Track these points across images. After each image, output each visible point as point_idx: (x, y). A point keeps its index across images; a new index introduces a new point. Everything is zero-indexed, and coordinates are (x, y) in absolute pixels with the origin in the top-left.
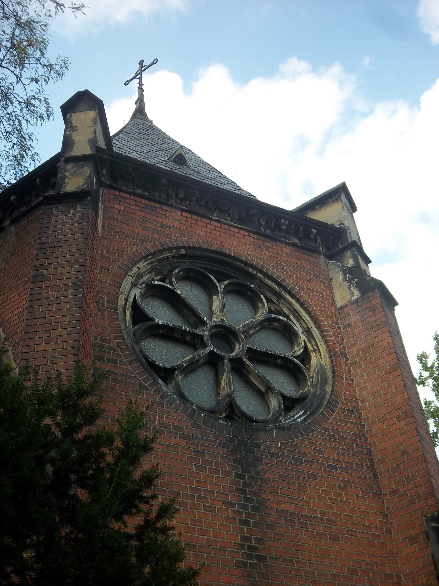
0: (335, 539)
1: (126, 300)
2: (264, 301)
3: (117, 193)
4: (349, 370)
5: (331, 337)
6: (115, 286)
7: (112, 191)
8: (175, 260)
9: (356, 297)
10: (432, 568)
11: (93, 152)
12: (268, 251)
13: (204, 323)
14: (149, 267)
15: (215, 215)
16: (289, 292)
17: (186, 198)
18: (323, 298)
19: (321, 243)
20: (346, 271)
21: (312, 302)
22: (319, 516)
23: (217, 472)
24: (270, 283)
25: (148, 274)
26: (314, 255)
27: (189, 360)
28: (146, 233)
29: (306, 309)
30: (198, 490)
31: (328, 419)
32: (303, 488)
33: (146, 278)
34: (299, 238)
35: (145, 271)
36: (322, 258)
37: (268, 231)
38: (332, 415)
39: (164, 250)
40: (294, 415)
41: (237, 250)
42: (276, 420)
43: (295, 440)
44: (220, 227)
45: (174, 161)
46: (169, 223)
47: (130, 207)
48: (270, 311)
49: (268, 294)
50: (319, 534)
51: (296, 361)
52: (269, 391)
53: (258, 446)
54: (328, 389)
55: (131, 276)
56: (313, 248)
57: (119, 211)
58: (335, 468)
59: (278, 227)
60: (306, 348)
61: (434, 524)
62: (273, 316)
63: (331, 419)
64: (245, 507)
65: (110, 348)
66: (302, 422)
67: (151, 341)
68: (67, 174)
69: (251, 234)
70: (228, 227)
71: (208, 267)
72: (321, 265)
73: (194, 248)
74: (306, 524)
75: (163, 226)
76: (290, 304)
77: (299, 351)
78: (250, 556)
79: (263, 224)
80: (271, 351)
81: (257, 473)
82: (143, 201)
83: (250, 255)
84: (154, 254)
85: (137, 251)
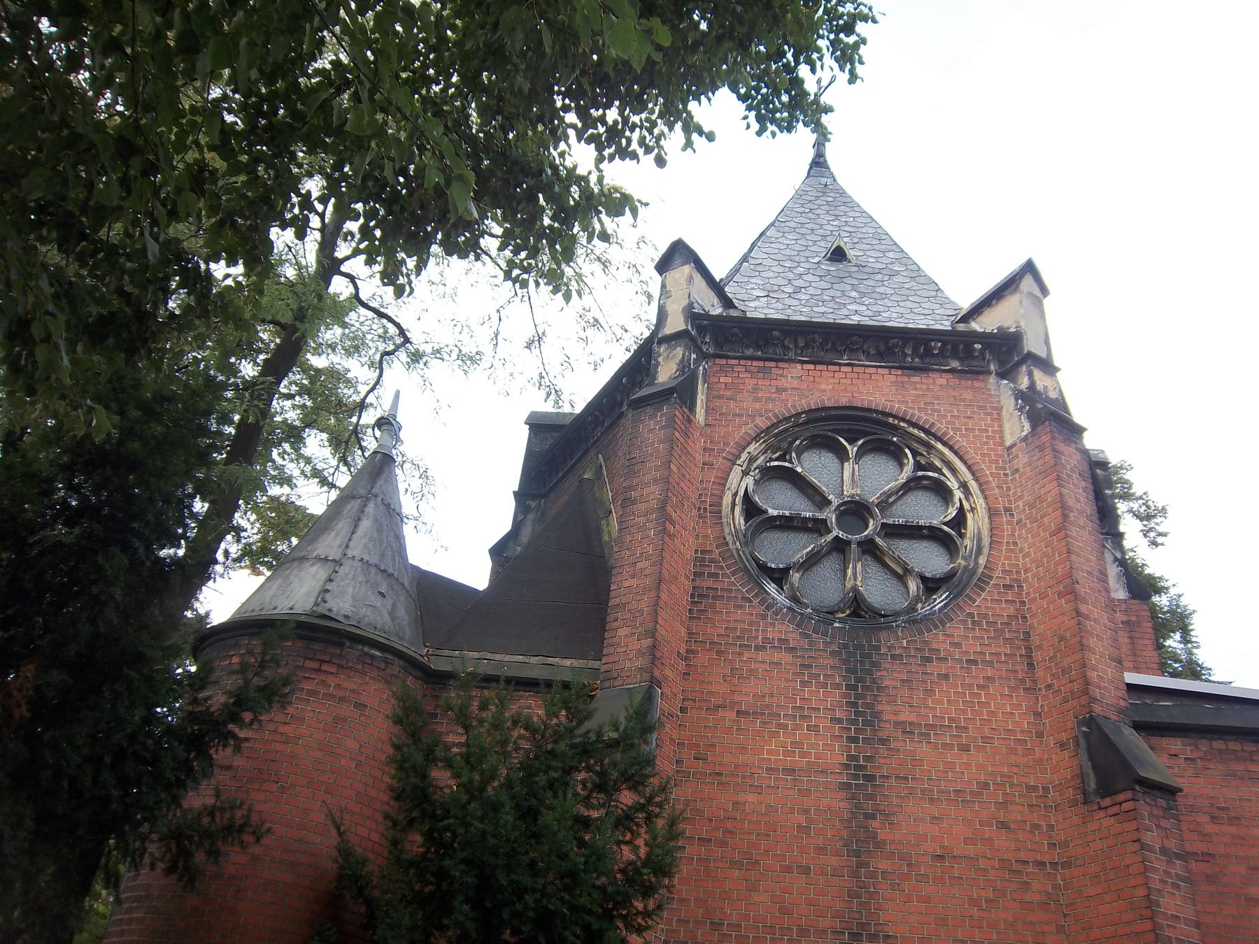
0: (965, 748)
1: (735, 495)
2: (910, 455)
3: (724, 362)
4: (1013, 530)
5: (993, 489)
7: (717, 361)
8: (796, 429)
9: (1024, 434)
10: (1079, 781)
12: (916, 389)
13: (829, 502)
14: (764, 445)
15: (845, 357)
16: (939, 439)
17: (807, 346)
18: (987, 437)
20: (1019, 395)
21: (970, 447)
23: (825, 685)
24: (915, 431)
26: (981, 377)
27: (807, 554)
28: (757, 406)
29: (961, 458)
30: (801, 708)
31: (975, 601)
33: (759, 461)
36: (992, 379)
37: (917, 360)
38: (980, 595)
39: (780, 422)
40: (935, 600)
42: (912, 608)
43: (926, 634)
45: (830, 259)
48: (918, 467)
49: (915, 445)
50: (945, 745)
51: (945, 528)
53: (878, 648)
54: (982, 561)
55: (739, 465)
56: (980, 369)
58: (975, 662)
59: (928, 352)
60: (961, 507)
61: (1084, 729)
62: (920, 473)
64: (855, 722)
68: (660, 359)
69: (893, 371)
71: (837, 427)
72: (989, 390)
73: (817, 410)
74: (928, 735)
75: (780, 390)
76: (942, 453)
77: (952, 512)
78: (856, 777)
79: (910, 352)
80: (912, 522)
82: (755, 363)
83: (890, 401)
85: (746, 433)
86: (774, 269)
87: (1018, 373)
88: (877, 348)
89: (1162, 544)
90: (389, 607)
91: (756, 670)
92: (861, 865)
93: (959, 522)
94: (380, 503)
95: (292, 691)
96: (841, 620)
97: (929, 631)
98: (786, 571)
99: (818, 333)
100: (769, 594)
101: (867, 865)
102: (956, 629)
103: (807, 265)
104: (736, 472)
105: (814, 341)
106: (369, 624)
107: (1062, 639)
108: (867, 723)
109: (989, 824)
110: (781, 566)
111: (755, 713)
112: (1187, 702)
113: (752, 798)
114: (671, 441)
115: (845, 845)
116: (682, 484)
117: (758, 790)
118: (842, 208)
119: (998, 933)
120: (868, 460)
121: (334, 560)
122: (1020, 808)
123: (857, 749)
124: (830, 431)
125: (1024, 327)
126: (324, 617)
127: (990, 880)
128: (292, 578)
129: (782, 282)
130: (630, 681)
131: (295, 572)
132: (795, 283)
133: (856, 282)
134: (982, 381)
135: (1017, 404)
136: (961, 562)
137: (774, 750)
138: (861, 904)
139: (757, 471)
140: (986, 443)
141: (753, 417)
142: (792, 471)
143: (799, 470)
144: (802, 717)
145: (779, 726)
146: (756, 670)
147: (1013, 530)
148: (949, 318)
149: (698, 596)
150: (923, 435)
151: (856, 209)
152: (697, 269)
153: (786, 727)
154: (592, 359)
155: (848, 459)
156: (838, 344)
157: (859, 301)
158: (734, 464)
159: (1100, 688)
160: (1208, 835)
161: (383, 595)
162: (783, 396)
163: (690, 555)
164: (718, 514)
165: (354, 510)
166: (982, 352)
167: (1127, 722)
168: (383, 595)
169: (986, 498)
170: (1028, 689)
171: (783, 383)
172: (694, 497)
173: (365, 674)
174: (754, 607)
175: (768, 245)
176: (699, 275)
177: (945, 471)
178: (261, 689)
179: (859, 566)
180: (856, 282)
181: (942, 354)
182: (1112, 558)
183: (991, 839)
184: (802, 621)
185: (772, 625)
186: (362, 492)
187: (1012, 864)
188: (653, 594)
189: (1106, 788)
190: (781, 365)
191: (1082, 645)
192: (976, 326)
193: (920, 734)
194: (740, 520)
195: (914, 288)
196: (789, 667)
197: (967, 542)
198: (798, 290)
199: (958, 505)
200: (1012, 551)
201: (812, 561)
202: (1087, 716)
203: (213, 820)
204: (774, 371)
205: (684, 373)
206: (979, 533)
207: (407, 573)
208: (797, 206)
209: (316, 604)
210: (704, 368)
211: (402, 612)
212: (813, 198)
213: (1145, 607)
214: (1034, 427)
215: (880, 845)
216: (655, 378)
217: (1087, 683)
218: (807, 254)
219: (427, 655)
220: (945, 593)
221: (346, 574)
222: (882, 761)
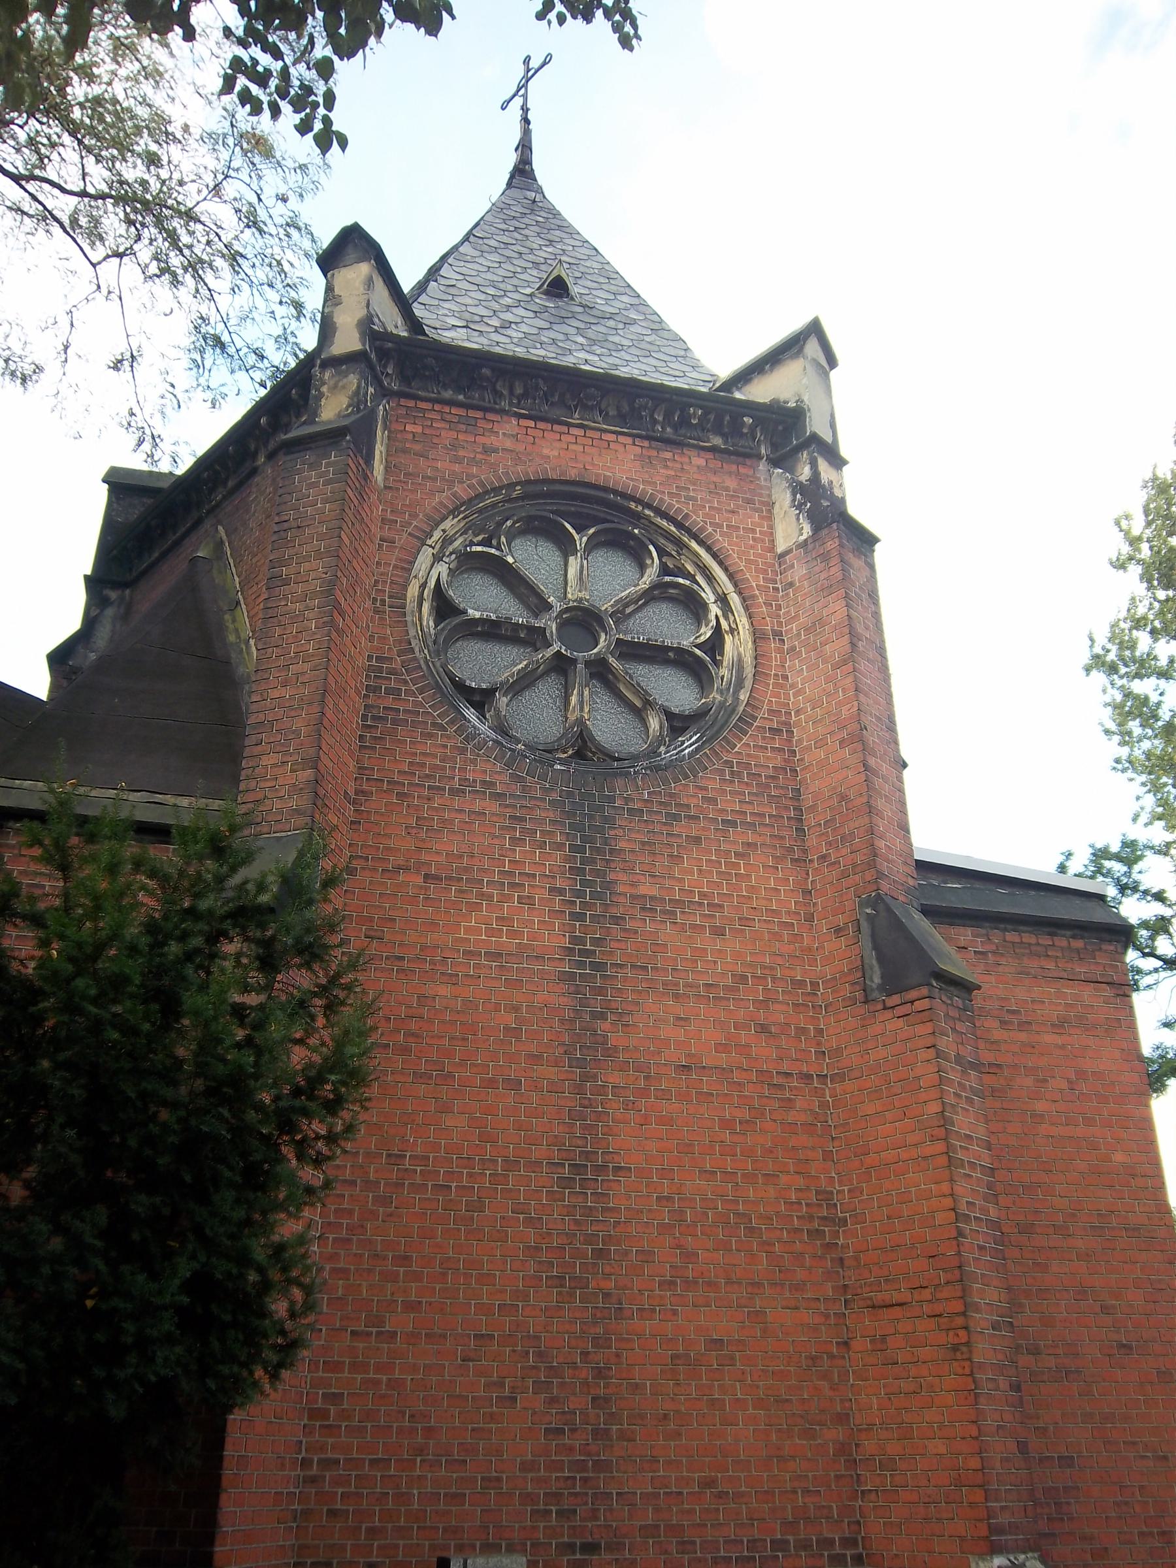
0: (718, 932)
1: (423, 586)
2: (655, 554)
3: (411, 403)
4: (783, 660)
6: (403, 568)
7: (403, 401)
9: (804, 537)
10: (859, 974)
11: (364, 345)
12: (666, 467)
13: (549, 607)
14: (462, 524)
15: (576, 416)
16: (695, 537)
17: (525, 395)
18: (754, 539)
19: (762, 438)
20: (798, 488)
21: (733, 550)
22: (697, 899)
25: (461, 535)
26: (748, 462)
28: (457, 467)
32: (676, 859)
33: (457, 544)
34: (724, 436)
35: (457, 533)
36: (763, 466)
37: (668, 429)
39: (487, 492)
40: (683, 743)
41: (608, 474)
42: (653, 752)
43: (673, 785)
44: (585, 436)
45: (547, 293)
46: (496, 444)
47: (432, 425)
48: (665, 570)
49: (662, 541)
50: (694, 927)
52: (648, 707)
53: (611, 799)
54: (743, 696)
55: (430, 546)
56: (748, 450)
57: (414, 436)
58: (733, 824)
59: (685, 422)
60: (718, 627)
61: (869, 911)
62: (667, 579)
63: (739, 746)
64: (580, 894)
65: (392, 672)
66: (691, 755)
67: (465, 644)
68: (324, 389)
70: (597, 435)
71: (562, 508)
72: (759, 479)
73: (537, 482)
74: (674, 913)
75: (487, 450)
77: (706, 633)
78: (581, 965)
79: (661, 419)
80: (656, 641)
81: (606, 842)
83: (632, 480)
84: (470, 502)
85: (441, 503)
86: (473, 294)
88: (618, 408)
91: (452, 821)
92: (585, 1078)
93: (715, 645)
96: (562, 762)
97: (676, 780)
99: (543, 378)
100: (470, 722)
101: (595, 1077)
103: (517, 296)
105: (537, 388)
109: (746, 1027)
111: (450, 878)
113: (445, 991)
115: (565, 1052)
116: (355, 563)
117: (453, 980)
118: (557, 233)
119: (754, 1162)
124: (553, 512)
125: (807, 403)
127: (746, 1097)
129: (484, 312)
130: (279, 827)
132: (502, 316)
133: (582, 326)
134: (751, 467)
135: (794, 500)
136: (715, 696)
138: (585, 1127)
139: (453, 556)
141: (451, 483)
143: (510, 560)
144: (513, 885)
145: (481, 895)
148: (706, 384)
149: (372, 719)
150: (673, 529)
151: (575, 236)
153: (490, 897)
156: (568, 396)
157: (588, 348)
158: (424, 544)
162: (493, 458)
163: (362, 661)
164: (400, 608)
166: (752, 429)
167: (915, 905)
169: (750, 617)
170: (796, 860)
172: (368, 582)
174: (448, 737)
175: (462, 264)
176: (380, 279)
177: (699, 578)
180: (582, 326)
181: (701, 426)
183: (748, 1046)
184: (513, 760)
185: (474, 762)
187: (772, 1077)
188: (316, 708)
189: (894, 983)
190: (490, 416)
191: (870, 807)
192: (738, 395)
193: (664, 912)
194: (428, 621)
195: (658, 343)
196: (495, 819)
197: (724, 672)
198: (506, 325)
199: (714, 623)
200: (782, 686)
201: (522, 684)
202: (873, 894)
205: (359, 410)
206: (740, 660)
208: (497, 221)
210: (385, 409)
212: (518, 215)
214: (816, 529)
215: (611, 1052)
216: (315, 414)
217: (875, 854)
218: (515, 281)
220: (695, 734)
222: (613, 944)
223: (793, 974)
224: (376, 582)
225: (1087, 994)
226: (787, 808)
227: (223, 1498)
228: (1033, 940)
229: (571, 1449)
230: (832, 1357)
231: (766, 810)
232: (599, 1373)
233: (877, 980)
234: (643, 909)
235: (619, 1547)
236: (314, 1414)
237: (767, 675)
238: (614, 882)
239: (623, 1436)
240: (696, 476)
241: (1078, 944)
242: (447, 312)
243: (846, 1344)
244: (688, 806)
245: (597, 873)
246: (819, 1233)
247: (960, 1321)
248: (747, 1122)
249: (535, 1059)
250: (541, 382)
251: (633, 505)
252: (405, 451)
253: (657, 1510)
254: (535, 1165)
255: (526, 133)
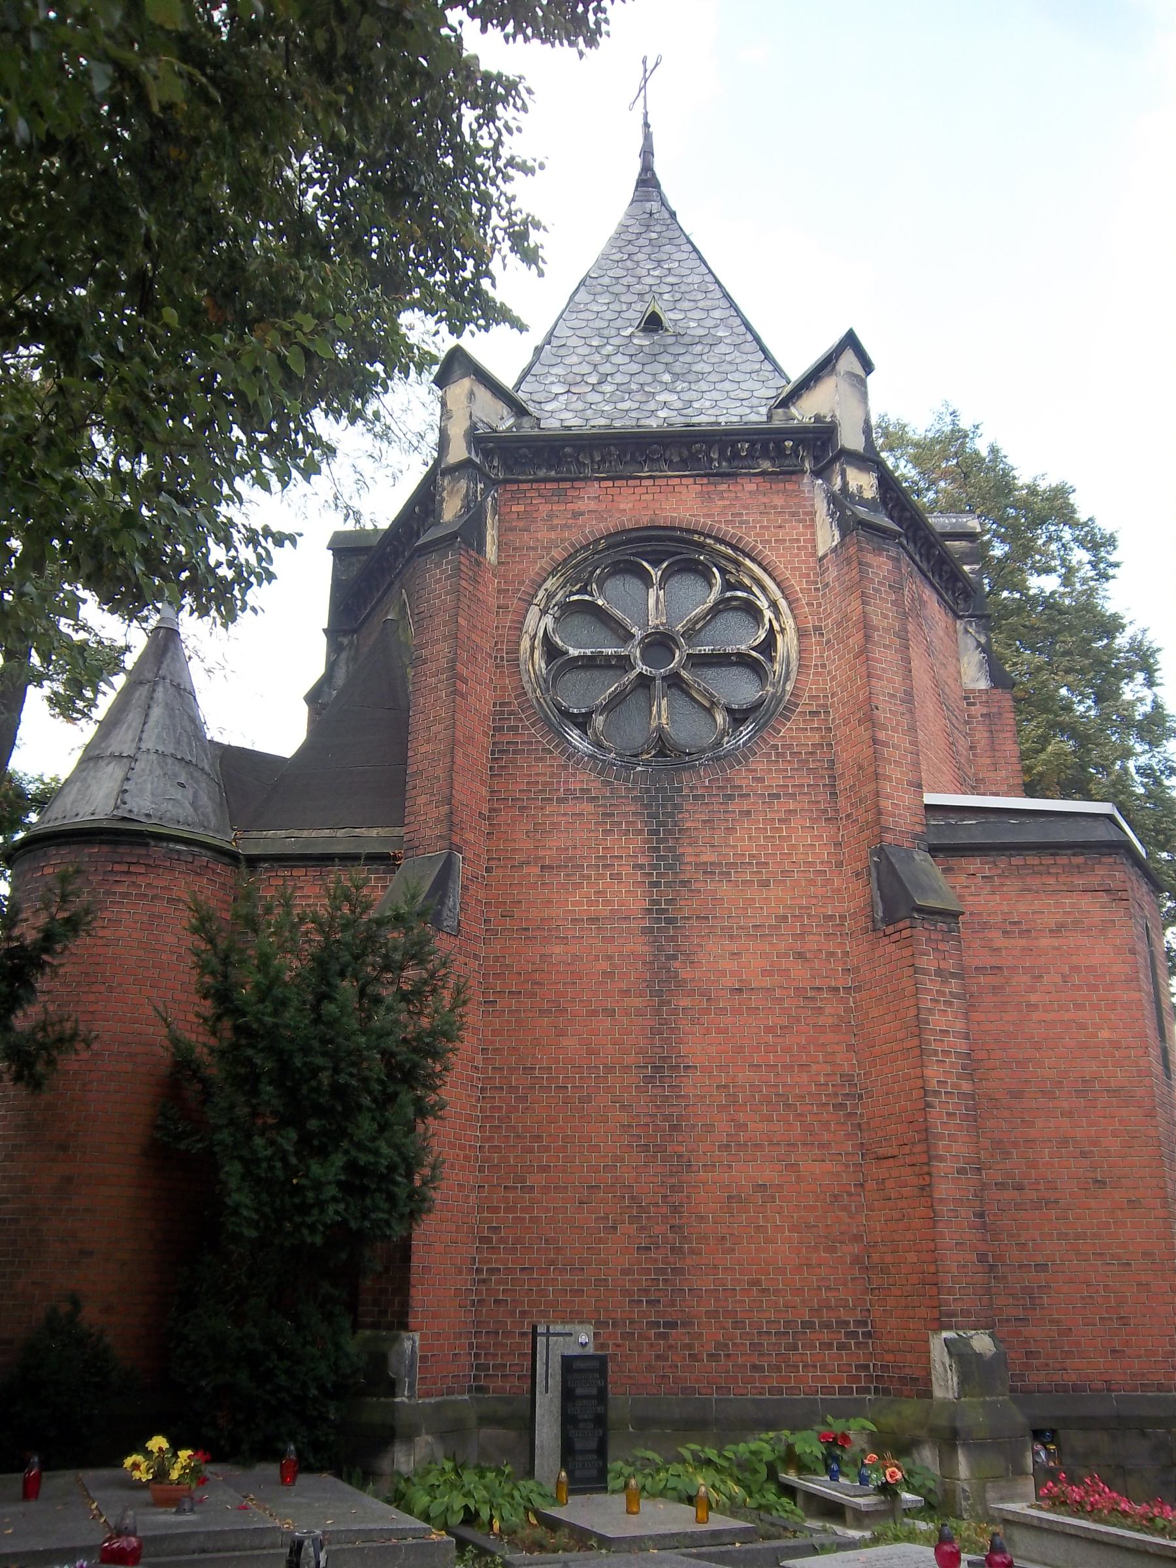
0: (765, 884)
3: (515, 487)
8: (596, 557)
9: (834, 544)
11: (470, 453)
12: (722, 498)
13: (633, 636)
15: (646, 469)
17: (603, 461)
18: (799, 548)
20: (832, 498)
26: (794, 478)
29: (770, 575)
30: (604, 857)
32: (730, 830)
33: (558, 597)
34: (772, 459)
38: (785, 725)
39: (577, 551)
42: (718, 744)
45: (644, 330)
46: (583, 508)
48: (728, 586)
50: (744, 882)
51: (754, 654)
53: (680, 789)
54: (789, 687)
58: (778, 796)
59: (736, 455)
60: (771, 631)
62: (728, 594)
64: (654, 867)
66: (745, 744)
72: (803, 492)
73: (617, 533)
74: (729, 873)
75: (576, 515)
77: (762, 635)
79: (716, 456)
83: (694, 516)
85: (542, 568)
87: (833, 471)
88: (680, 455)
89: (1113, 577)
90: (191, 797)
91: (559, 823)
92: (662, 1003)
93: (768, 646)
94: (168, 685)
95: (94, 919)
96: (647, 763)
97: (731, 767)
98: (589, 714)
99: (613, 445)
100: (570, 743)
101: (669, 1002)
102: (759, 764)
104: (534, 611)
106: (171, 819)
107: (860, 767)
108: (669, 867)
109: (787, 955)
110: (583, 711)
112: (992, 818)
113: (558, 949)
114: (457, 591)
116: (473, 636)
120: (675, 582)
121: (129, 756)
122: (817, 938)
123: (659, 893)
124: (632, 554)
126: (124, 819)
128: (89, 780)
130: (431, 849)
131: (92, 773)
136: (770, 689)
137: (578, 902)
138: (661, 1039)
140: (797, 555)
141: (548, 549)
142: (593, 604)
143: (600, 602)
144: (605, 866)
145: (583, 876)
146: (559, 823)
147: (822, 652)
149: (499, 752)
150: (730, 551)
152: (479, 381)
153: (589, 877)
154: (389, 471)
155: (652, 585)
158: (531, 604)
159: (894, 816)
160: (998, 949)
161: (182, 785)
164: (515, 662)
165: (143, 698)
166: (795, 450)
167: (922, 847)
168: (182, 785)
169: (795, 617)
171: (580, 505)
172: (487, 646)
173: (172, 870)
174: (554, 758)
177: (755, 589)
178: (67, 921)
179: (664, 702)
181: (751, 455)
182: (975, 644)
185: (574, 775)
186: (149, 676)
188: (448, 759)
190: (577, 484)
191: (877, 775)
193: (720, 873)
194: (540, 662)
195: (738, 361)
196: (591, 817)
197: (777, 667)
199: (767, 626)
200: (820, 674)
203: (47, 1035)
204: (570, 493)
205: (468, 509)
206: (788, 656)
207: (206, 755)
209: (117, 807)
210: (494, 498)
211: (204, 800)
213: (1008, 696)
214: (843, 536)
215: (680, 983)
216: (440, 517)
217: (880, 813)
219: (235, 839)
221: (143, 770)
222: (683, 903)
223: (824, 910)
224: (496, 643)
225: (1085, 902)
226: (823, 777)
227: (413, 1292)
228: (1037, 862)
229: (656, 1261)
230: (850, 1194)
231: (805, 781)
232: (675, 1209)
233: (881, 914)
234: (705, 873)
235: (691, 1324)
236: (484, 1240)
237: (807, 666)
238: (683, 854)
239: (692, 1251)
240: (748, 501)
241: (1079, 860)
242: (553, 379)
243: (862, 1185)
244: (741, 787)
245: (669, 849)
246: (842, 1106)
247: (926, 1169)
248: (786, 1027)
249: (626, 993)
250: (612, 448)
251: (696, 537)
252: (512, 529)
253: (717, 1300)
254: (628, 1068)
255: (648, 137)
